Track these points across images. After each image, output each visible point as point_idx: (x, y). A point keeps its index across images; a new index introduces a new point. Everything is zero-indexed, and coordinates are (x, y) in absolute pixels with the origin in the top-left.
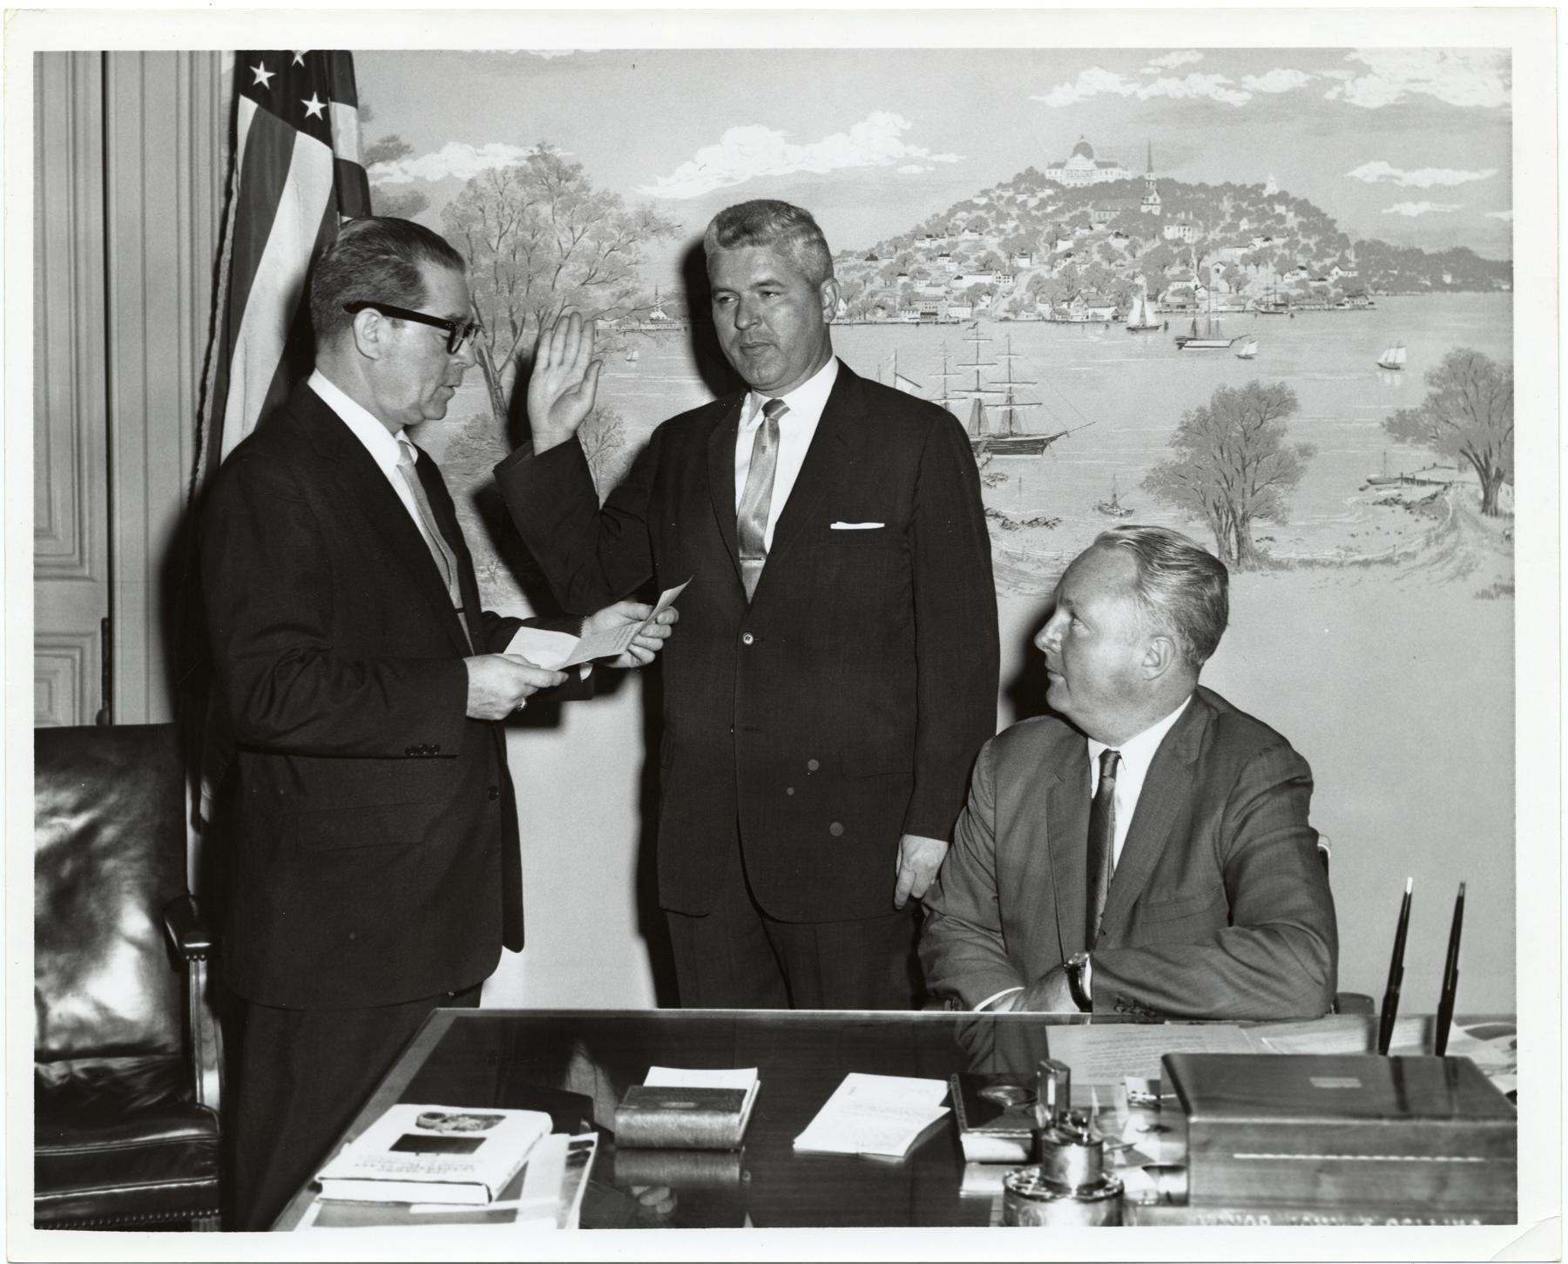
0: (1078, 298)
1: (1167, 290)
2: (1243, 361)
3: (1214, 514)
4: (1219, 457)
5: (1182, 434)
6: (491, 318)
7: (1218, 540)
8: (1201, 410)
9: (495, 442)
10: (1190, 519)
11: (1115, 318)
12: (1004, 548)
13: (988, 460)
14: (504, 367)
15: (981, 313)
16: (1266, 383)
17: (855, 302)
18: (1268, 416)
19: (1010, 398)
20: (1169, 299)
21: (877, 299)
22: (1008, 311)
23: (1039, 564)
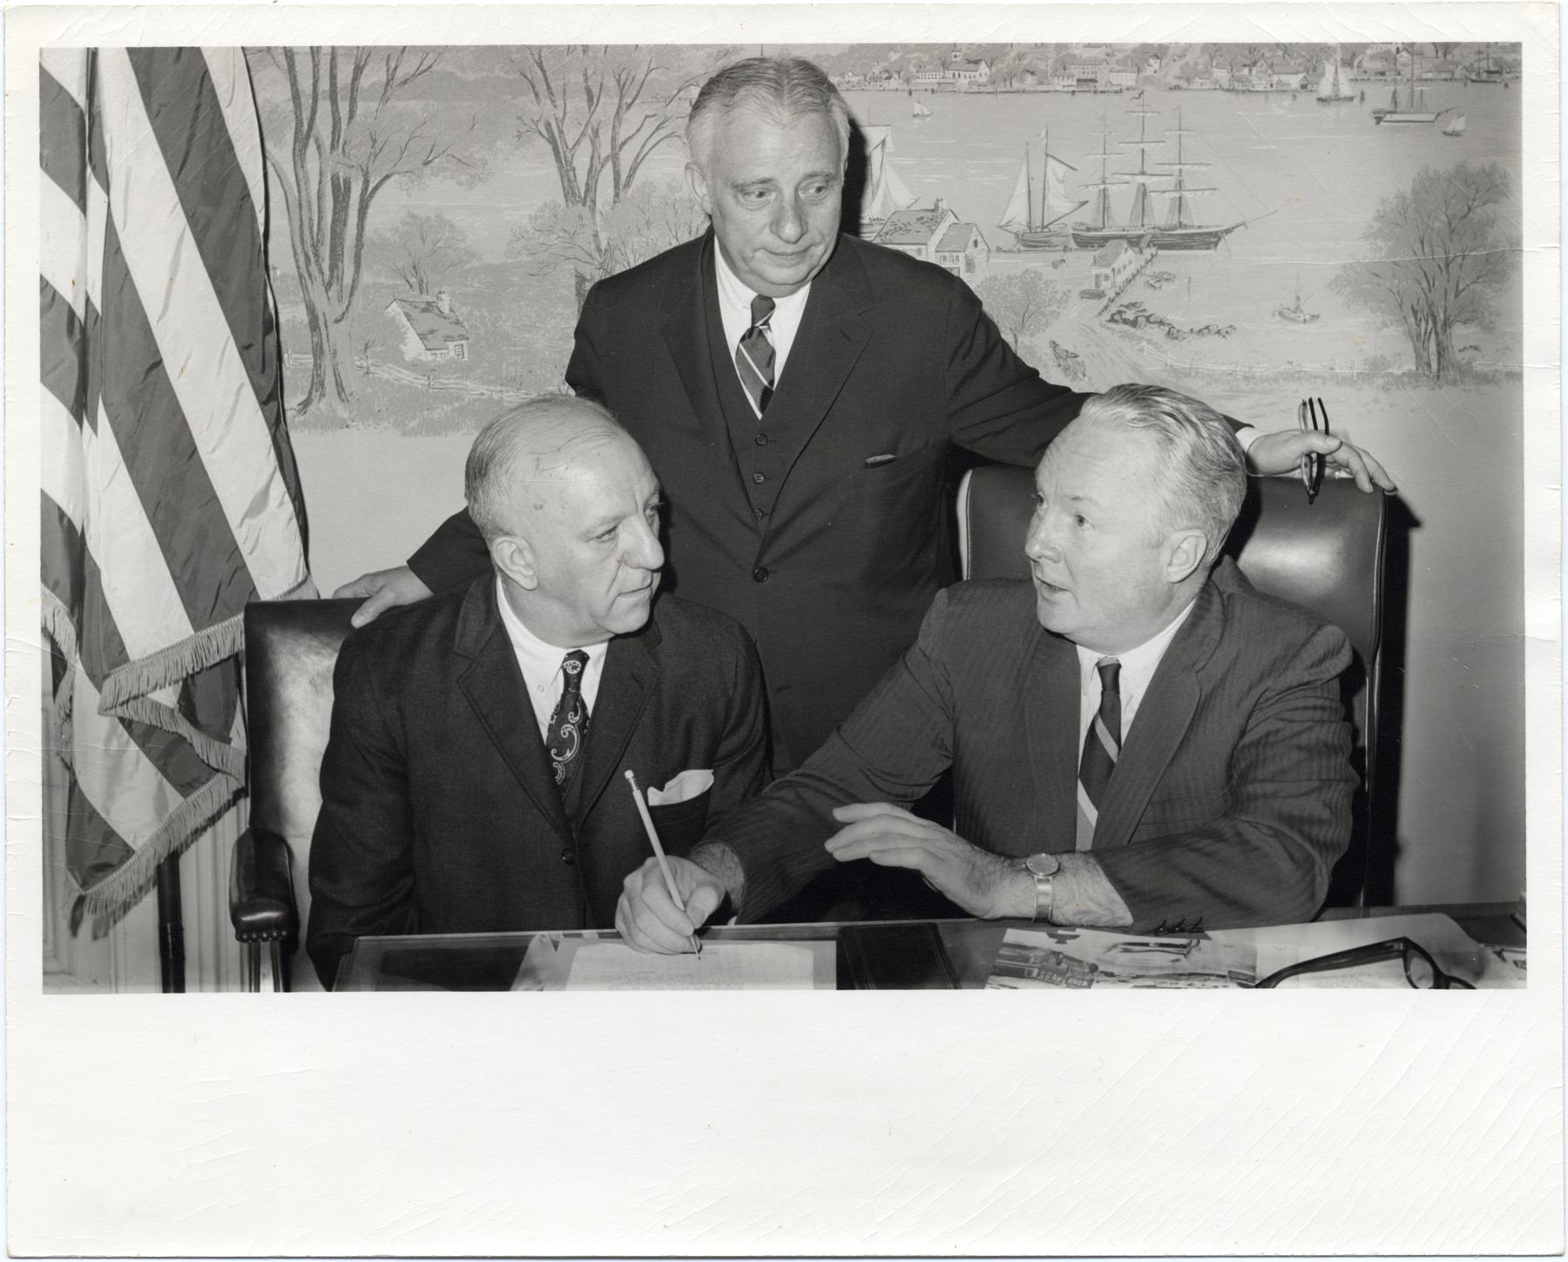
0: (1258, 64)
1: (1365, 53)
2: (1448, 137)
3: (1412, 320)
4: (1419, 252)
5: (1375, 224)
6: (561, 83)
7: (1416, 350)
8: (1401, 196)
9: (567, 235)
10: (1385, 325)
11: (1304, 87)
12: (1169, 362)
13: (1152, 256)
14: (577, 143)
15: (1148, 80)
16: (1476, 164)
17: (1000, 66)
18: (1476, 203)
19: (1180, 182)
20: (1367, 65)
21: (1025, 62)
22: (1180, 78)
23: (1209, 379)
